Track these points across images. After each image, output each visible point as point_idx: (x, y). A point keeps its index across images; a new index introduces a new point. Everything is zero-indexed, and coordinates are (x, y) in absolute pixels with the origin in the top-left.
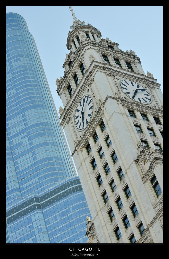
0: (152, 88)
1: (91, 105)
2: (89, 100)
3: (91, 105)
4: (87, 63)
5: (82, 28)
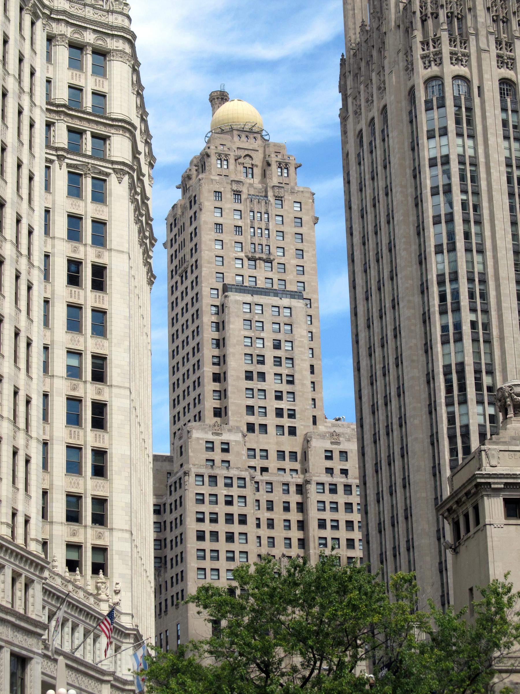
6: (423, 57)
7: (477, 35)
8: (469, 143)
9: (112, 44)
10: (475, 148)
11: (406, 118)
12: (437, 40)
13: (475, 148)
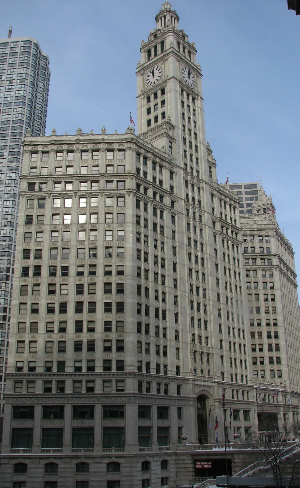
0: (197, 76)
1: (160, 74)
2: (160, 71)
3: (160, 74)
4: (167, 46)
5: (170, 12)
9: (271, 233)
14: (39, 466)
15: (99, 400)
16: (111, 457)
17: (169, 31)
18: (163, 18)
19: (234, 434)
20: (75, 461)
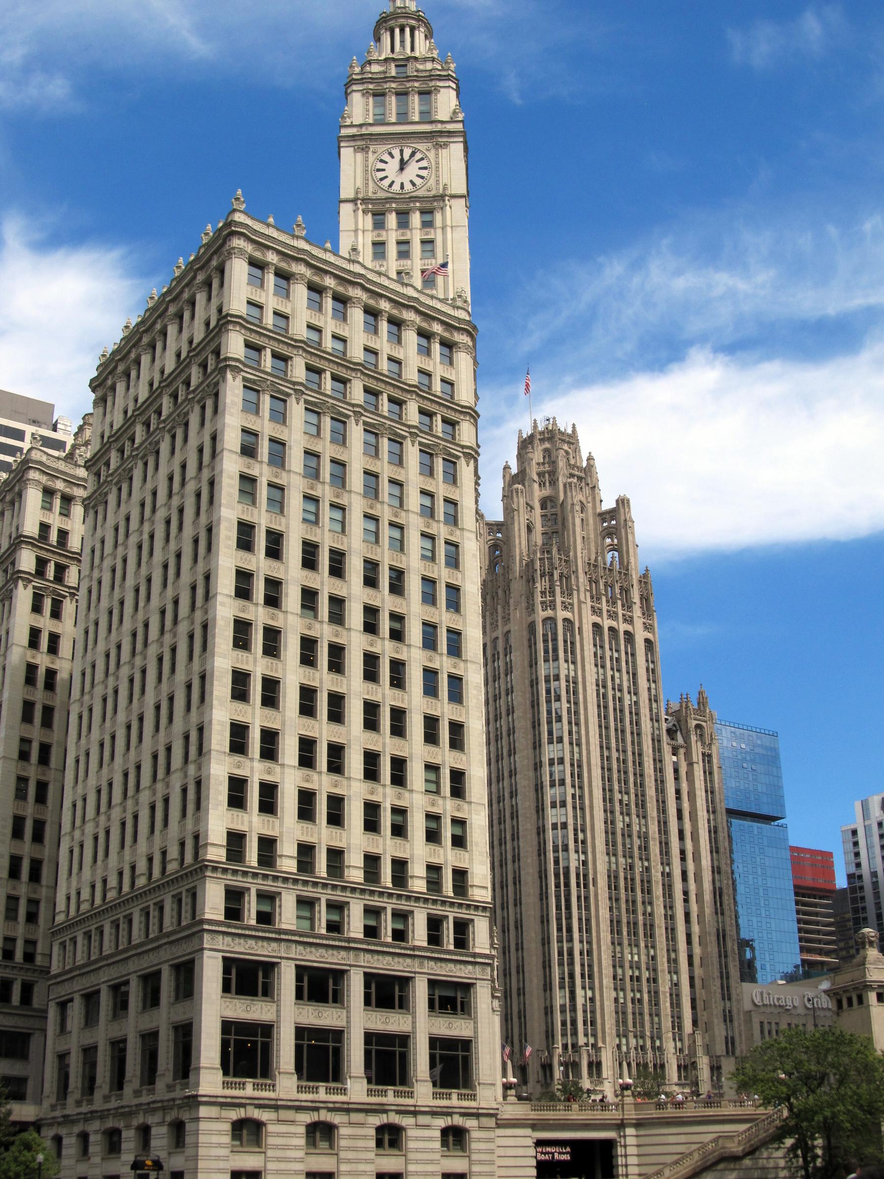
6: (542, 603)
7: (578, 591)
8: (572, 667)
10: (576, 671)
11: (526, 643)
12: (552, 592)
13: (576, 671)
14: (292, 1129)
15: (421, 965)
16: (450, 1114)
17: (448, 78)
18: (407, 30)
19: (621, 1081)
20: (376, 1120)
